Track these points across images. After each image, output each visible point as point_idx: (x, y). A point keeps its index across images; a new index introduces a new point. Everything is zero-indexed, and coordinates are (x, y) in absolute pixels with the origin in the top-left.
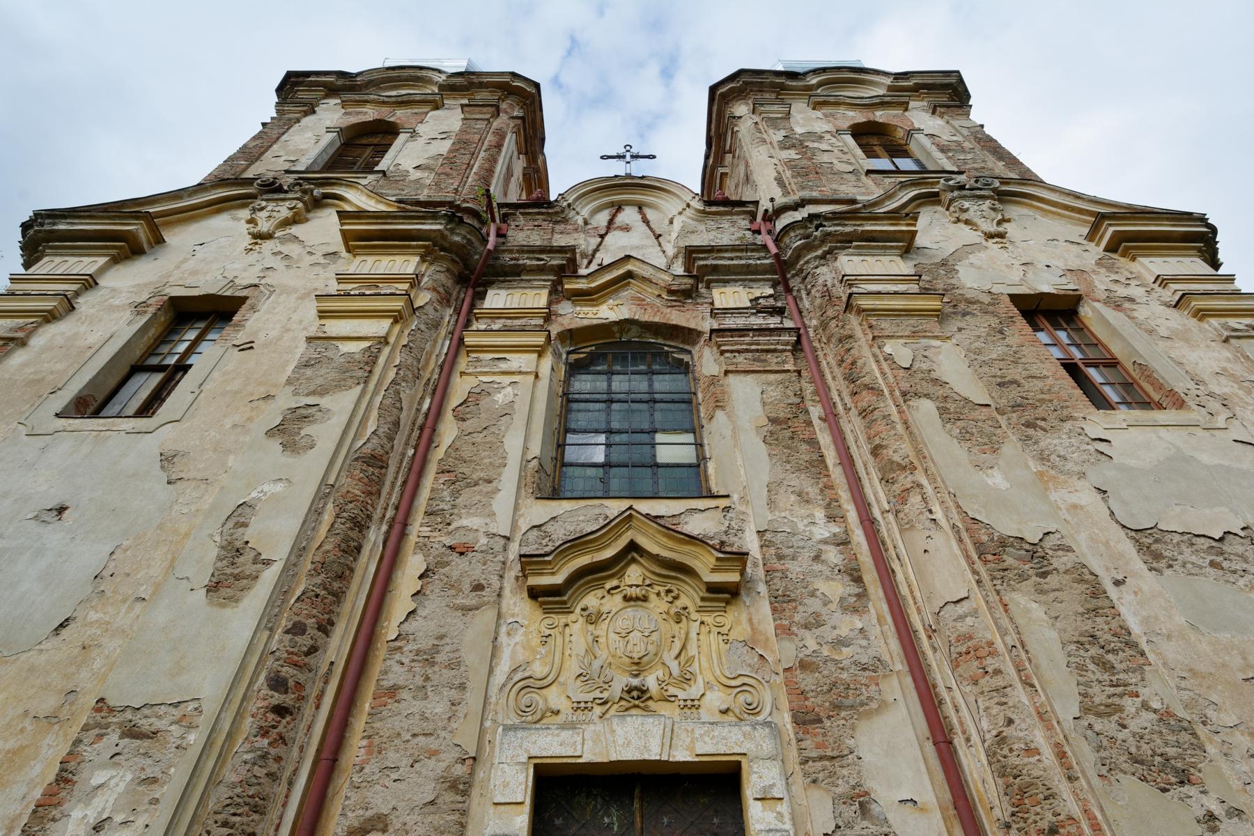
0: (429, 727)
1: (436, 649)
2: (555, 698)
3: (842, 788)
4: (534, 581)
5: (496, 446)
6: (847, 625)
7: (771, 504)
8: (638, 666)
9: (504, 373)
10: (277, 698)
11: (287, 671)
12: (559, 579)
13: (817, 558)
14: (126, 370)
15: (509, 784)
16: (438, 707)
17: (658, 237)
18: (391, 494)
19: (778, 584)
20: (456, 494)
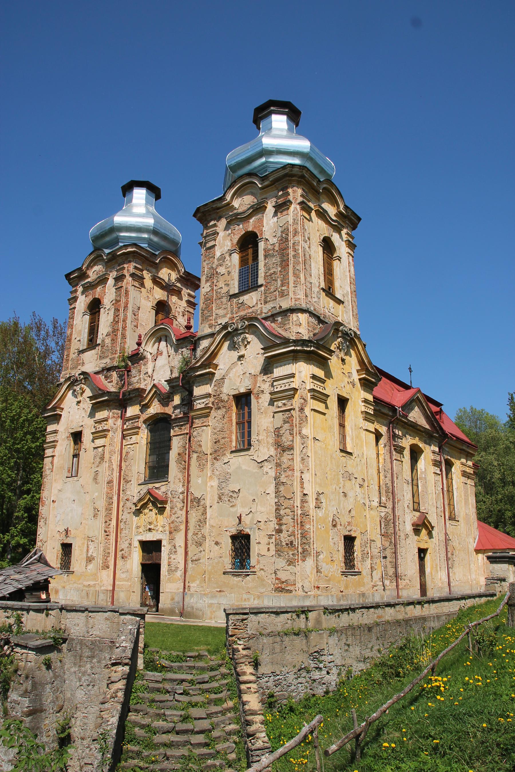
0: (126, 535)
1: (126, 522)
2: (141, 530)
3: (173, 544)
6: (179, 513)
8: (150, 523)
9: (131, 444)
10: (106, 534)
11: (107, 529)
13: (178, 498)
14: (72, 457)
15: (137, 544)
16: (127, 532)
18: (116, 488)
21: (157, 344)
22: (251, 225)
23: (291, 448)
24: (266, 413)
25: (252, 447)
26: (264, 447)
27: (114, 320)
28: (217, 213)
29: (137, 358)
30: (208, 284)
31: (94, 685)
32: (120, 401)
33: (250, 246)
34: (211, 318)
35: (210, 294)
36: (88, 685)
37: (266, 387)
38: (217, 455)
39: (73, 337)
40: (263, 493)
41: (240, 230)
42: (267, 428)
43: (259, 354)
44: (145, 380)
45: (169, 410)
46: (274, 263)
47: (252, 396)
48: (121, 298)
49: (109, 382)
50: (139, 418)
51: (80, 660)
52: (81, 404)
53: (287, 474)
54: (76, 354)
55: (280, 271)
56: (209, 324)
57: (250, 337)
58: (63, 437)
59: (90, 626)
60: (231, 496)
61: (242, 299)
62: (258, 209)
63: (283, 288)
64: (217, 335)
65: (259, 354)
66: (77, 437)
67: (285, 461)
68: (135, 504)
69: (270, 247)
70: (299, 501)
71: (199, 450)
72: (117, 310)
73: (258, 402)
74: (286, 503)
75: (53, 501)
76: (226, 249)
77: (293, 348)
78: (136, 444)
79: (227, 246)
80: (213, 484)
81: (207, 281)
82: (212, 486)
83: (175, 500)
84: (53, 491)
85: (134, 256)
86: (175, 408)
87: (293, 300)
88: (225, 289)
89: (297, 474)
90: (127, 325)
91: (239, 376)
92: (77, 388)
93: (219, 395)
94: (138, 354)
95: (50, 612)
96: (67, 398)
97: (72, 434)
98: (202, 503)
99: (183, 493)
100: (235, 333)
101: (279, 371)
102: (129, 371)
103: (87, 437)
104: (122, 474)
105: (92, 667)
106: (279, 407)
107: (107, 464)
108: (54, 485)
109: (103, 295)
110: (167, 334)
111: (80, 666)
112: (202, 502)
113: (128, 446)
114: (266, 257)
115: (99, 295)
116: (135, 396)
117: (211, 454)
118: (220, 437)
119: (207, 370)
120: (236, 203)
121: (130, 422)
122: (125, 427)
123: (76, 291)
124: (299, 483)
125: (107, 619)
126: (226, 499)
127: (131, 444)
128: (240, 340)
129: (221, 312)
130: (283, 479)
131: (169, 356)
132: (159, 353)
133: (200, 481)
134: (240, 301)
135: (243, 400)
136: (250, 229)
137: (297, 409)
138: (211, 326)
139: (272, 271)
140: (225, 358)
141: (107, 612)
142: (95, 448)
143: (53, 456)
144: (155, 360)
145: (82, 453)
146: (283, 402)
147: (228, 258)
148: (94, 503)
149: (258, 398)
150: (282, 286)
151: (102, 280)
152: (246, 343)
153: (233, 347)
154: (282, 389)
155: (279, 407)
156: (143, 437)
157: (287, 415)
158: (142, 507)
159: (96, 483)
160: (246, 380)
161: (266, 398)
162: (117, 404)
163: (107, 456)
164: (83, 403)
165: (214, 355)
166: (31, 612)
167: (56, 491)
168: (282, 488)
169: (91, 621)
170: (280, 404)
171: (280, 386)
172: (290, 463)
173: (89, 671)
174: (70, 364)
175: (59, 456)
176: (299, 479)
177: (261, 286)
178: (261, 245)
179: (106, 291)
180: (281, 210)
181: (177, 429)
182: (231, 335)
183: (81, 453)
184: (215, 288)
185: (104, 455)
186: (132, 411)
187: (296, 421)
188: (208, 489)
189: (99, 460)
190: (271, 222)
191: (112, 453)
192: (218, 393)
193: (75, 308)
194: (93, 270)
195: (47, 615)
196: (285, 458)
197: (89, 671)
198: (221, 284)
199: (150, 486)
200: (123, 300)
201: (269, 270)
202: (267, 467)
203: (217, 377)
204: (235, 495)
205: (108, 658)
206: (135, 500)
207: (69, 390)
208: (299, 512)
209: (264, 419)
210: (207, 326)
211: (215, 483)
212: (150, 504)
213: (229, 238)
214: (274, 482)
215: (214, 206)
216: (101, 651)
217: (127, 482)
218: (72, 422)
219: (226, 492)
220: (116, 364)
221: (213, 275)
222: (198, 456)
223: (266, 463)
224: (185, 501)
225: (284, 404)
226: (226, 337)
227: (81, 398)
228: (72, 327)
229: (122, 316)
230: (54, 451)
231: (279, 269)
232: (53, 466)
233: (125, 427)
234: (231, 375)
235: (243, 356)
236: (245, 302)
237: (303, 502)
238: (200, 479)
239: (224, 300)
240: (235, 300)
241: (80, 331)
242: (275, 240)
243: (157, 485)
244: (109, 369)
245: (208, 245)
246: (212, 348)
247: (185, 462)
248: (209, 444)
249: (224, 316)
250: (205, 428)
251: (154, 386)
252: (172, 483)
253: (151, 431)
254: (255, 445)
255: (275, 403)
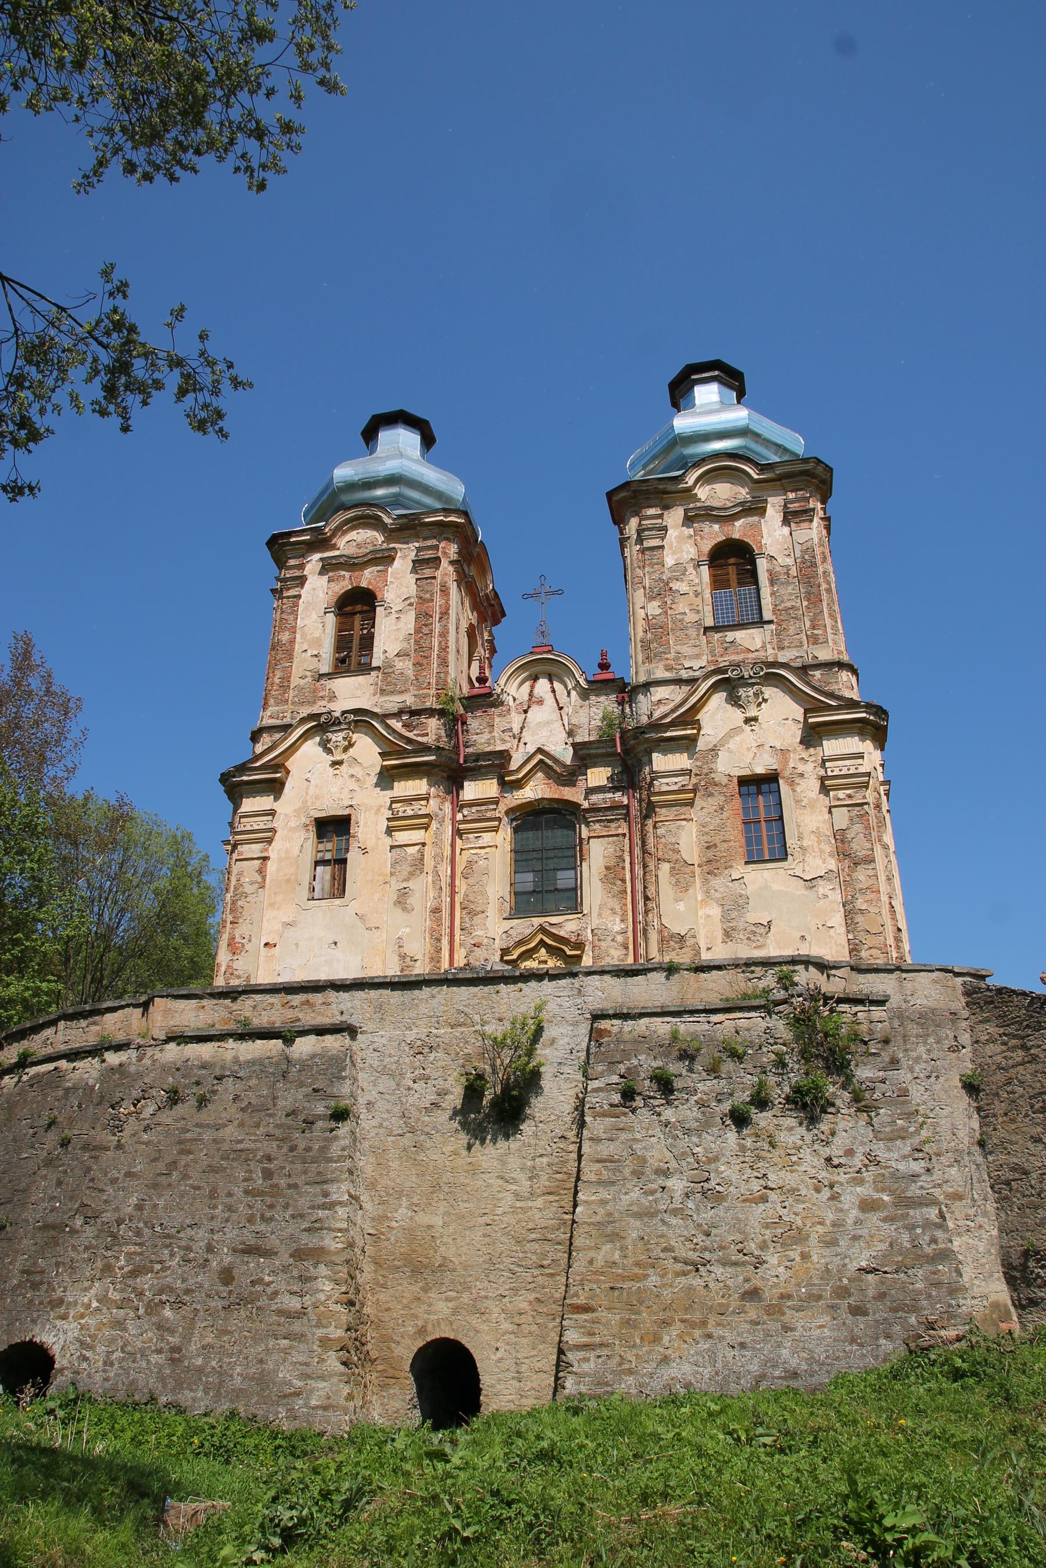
4: (505, 958)
5: (483, 893)
7: (600, 915)
9: (481, 848)
12: (515, 957)
13: (613, 940)
17: (561, 708)
19: (597, 952)
20: (471, 919)
21: (528, 684)
22: (738, 529)
23: (870, 860)
24: (812, 807)
25: (790, 857)
26: (814, 857)
27: (418, 630)
28: (662, 498)
29: (483, 700)
30: (656, 603)
31: (937, 1077)
32: (451, 771)
33: (732, 561)
34: (668, 656)
35: (662, 618)
36: (929, 1077)
37: (811, 771)
38: (713, 864)
39: (298, 648)
40: (820, 926)
41: (714, 534)
42: (818, 828)
43: (787, 719)
44: (504, 741)
45: (574, 794)
46: (791, 594)
47: (781, 781)
48: (432, 595)
49: (417, 735)
50: (497, 803)
51: (905, 1041)
52: (344, 768)
53: (867, 898)
54: (309, 679)
55: (807, 607)
56: (665, 666)
57: (769, 692)
58: (292, 824)
59: (909, 993)
60: (754, 933)
61: (730, 636)
62: (755, 508)
63: (815, 632)
64: (703, 681)
65: (787, 719)
66: (334, 827)
67: (862, 877)
68: (505, 951)
69: (778, 569)
70: (892, 939)
71: (675, 857)
72: (423, 617)
73: (794, 791)
74: (870, 940)
75: (266, 944)
76: (686, 557)
77: (864, 715)
78: (494, 849)
79: (688, 552)
80: (710, 913)
81: (652, 598)
82: (708, 916)
83: (602, 943)
84: (265, 924)
85: (458, 532)
86: (590, 791)
87: (836, 652)
88: (691, 617)
89: (884, 898)
90: (450, 644)
91: (749, 749)
92: (337, 738)
93: (707, 774)
94: (490, 695)
95: (833, 972)
96: (298, 753)
97: (316, 819)
98: (688, 943)
99: (624, 932)
100: (742, 681)
101: (832, 746)
102: (464, 723)
103: (369, 828)
104: (458, 899)
105: (929, 1051)
106: (839, 799)
107: (430, 879)
108: (269, 914)
109: (380, 585)
110: (554, 669)
111: (906, 1050)
112: (690, 942)
113: (472, 851)
114: (772, 583)
115: (370, 583)
116: (496, 765)
117: (699, 866)
118: (717, 840)
119: (689, 732)
120: (702, 493)
121: (474, 809)
122: (459, 817)
123: (301, 567)
124: (889, 916)
125: (935, 981)
126: (741, 936)
127: (481, 848)
128: (751, 693)
129: (686, 650)
130: (860, 904)
131: (561, 708)
132: (533, 700)
133: (681, 906)
134: (728, 639)
135: (760, 785)
136: (736, 536)
137: (872, 806)
138: (669, 668)
139: (789, 604)
140: (717, 717)
141: (933, 971)
142: (392, 847)
143: (265, 859)
144: (526, 712)
145: (353, 857)
146: (848, 792)
147: (691, 570)
148: (400, 947)
149: (792, 784)
150: (814, 629)
151: (385, 559)
152: (760, 700)
153: (734, 701)
154: (842, 773)
155: (839, 799)
156: (503, 838)
157: (856, 810)
158: (520, 956)
159: (405, 909)
160: (766, 756)
161: (810, 787)
162: (445, 775)
163: (429, 863)
164: (350, 766)
165: (695, 709)
166: (811, 968)
167: (278, 927)
168: (859, 918)
169: (908, 985)
170: (841, 794)
171: (835, 768)
172: (871, 882)
173: (925, 1056)
174: (291, 695)
175: (280, 860)
176: (887, 906)
177: (770, 622)
178: (762, 565)
179: (389, 579)
180: (797, 520)
181: (597, 826)
182: (730, 684)
183: (349, 856)
184: (669, 612)
185: (422, 860)
186: (471, 790)
187: (873, 821)
188: (701, 921)
189: (410, 869)
190: (777, 533)
191: (438, 857)
192: (705, 771)
193: (299, 597)
194: (348, 538)
195: (828, 976)
196: (861, 875)
197: (925, 1056)
198: (682, 606)
199: (537, 921)
200: (438, 601)
201: (782, 602)
202: (823, 888)
203: (701, 745)
204: (762, 930)
205: (951, 1036)
206: (498, 944)
207: (306, 740)
208: (895, 955)
209: (807, 816)
210: (661, 665)
211: (715, 911)
212: (543, 951)
213: (692, 541)
214: (842, 909)
215: (661, 487)
216: (938, 1026)
217: (472, 913)
218: (317, 797)
219: (741, 925)
220: (431, 703)
221: (662, 592)
222: (674, 868)
223: (820, 882)
224: (631, 947)
225: (850, 796)
226: (715, 688)
227: (344, 757)
228: (293, 630)
229: (437, 628)
230: (266, 850)
231: (805, 603)
232: (264, 878)
233: (459, 817)
234: (732, 745)
235: (755, 719)
236: (738, 641)
237: (898, 940)
238: (681, 903)
239: (693, 633)
240: (717, 636)
241: (318, 642)
242: (790, 561)
243: (554, 920)
244: (413, 713)
245: (647, 544)
246: (693, 700)
247: (623, 881)
248: (696, 851)
249: (698, 656)
250: (684, 823)
251: (540, 750)
252: (595, 915)
253: (516, 830)
254: (796, 854)
255: (831, 793)
